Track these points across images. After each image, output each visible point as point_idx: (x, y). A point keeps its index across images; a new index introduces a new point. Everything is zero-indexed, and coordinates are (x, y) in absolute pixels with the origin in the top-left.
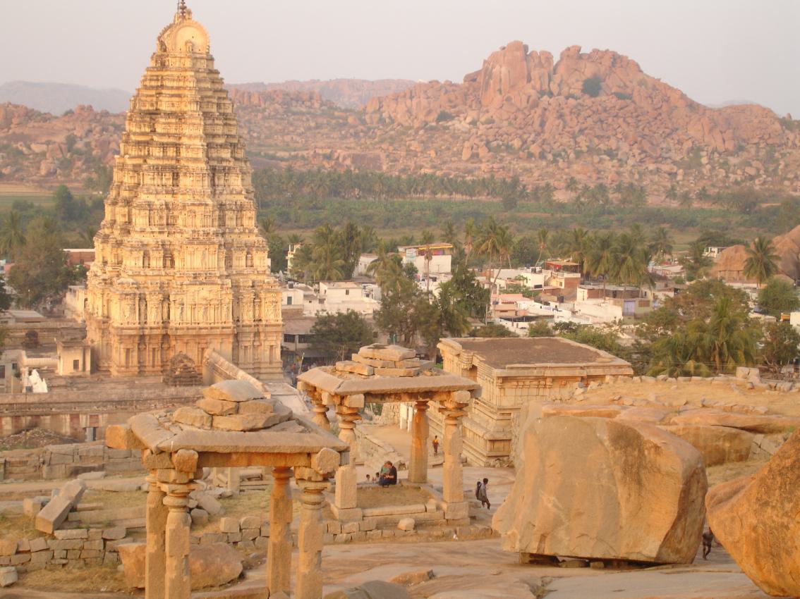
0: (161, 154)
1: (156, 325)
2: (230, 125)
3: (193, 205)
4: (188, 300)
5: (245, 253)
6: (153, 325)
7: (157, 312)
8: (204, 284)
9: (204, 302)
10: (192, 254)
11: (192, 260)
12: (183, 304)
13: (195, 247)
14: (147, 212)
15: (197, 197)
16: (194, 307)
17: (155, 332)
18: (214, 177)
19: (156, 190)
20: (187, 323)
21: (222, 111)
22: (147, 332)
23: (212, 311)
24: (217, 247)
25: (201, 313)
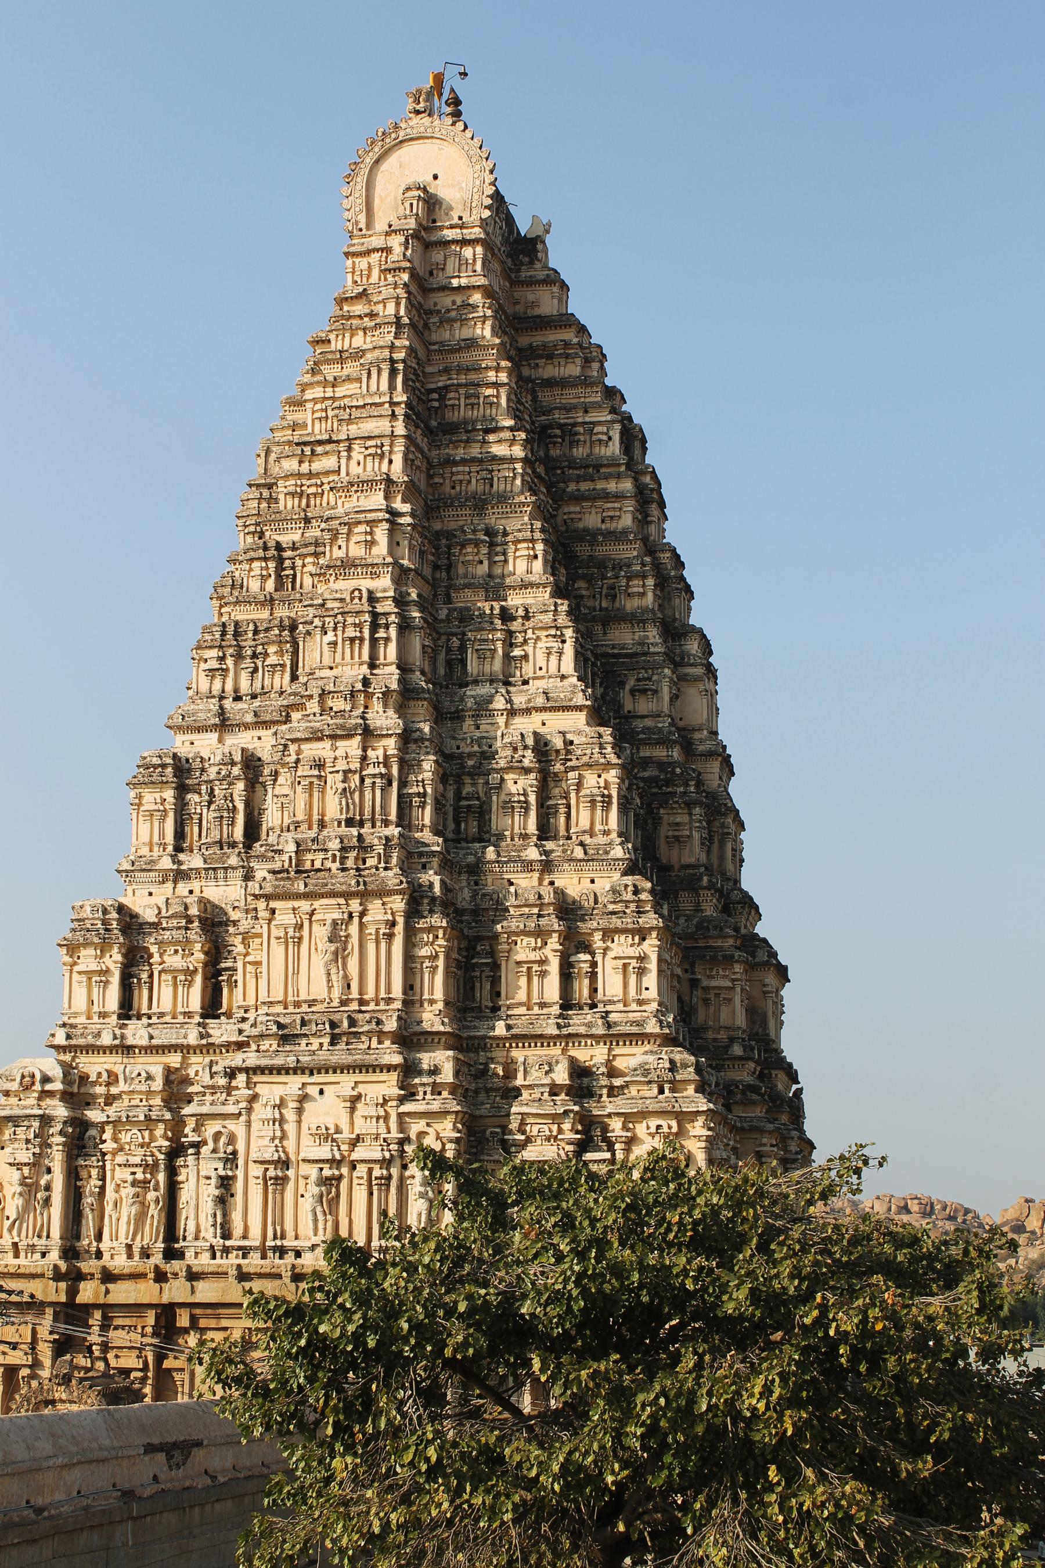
0: (270, 585)
1: (137, 1263)
2: (606, 496)
3: (317, 736)
4: (259, 1144)
5: (554, 942)
6: (120, 1262)
7: (139, 1200)
8: (326, 1069)
9: (325, 1152)
10: (295, 939)
11: (287, 967)
12: (231, 1159)
13: (305, 905)
14: (169, 794)
15: (338, 704)
16: (279, 1171)
17: (122, 1293)
18: (463, 649)
19: (222, 712)
20: (245, 1252)
22: (88, 1292)
23: (360, 1195)
24: (398, 904)
25: (307, 1204)
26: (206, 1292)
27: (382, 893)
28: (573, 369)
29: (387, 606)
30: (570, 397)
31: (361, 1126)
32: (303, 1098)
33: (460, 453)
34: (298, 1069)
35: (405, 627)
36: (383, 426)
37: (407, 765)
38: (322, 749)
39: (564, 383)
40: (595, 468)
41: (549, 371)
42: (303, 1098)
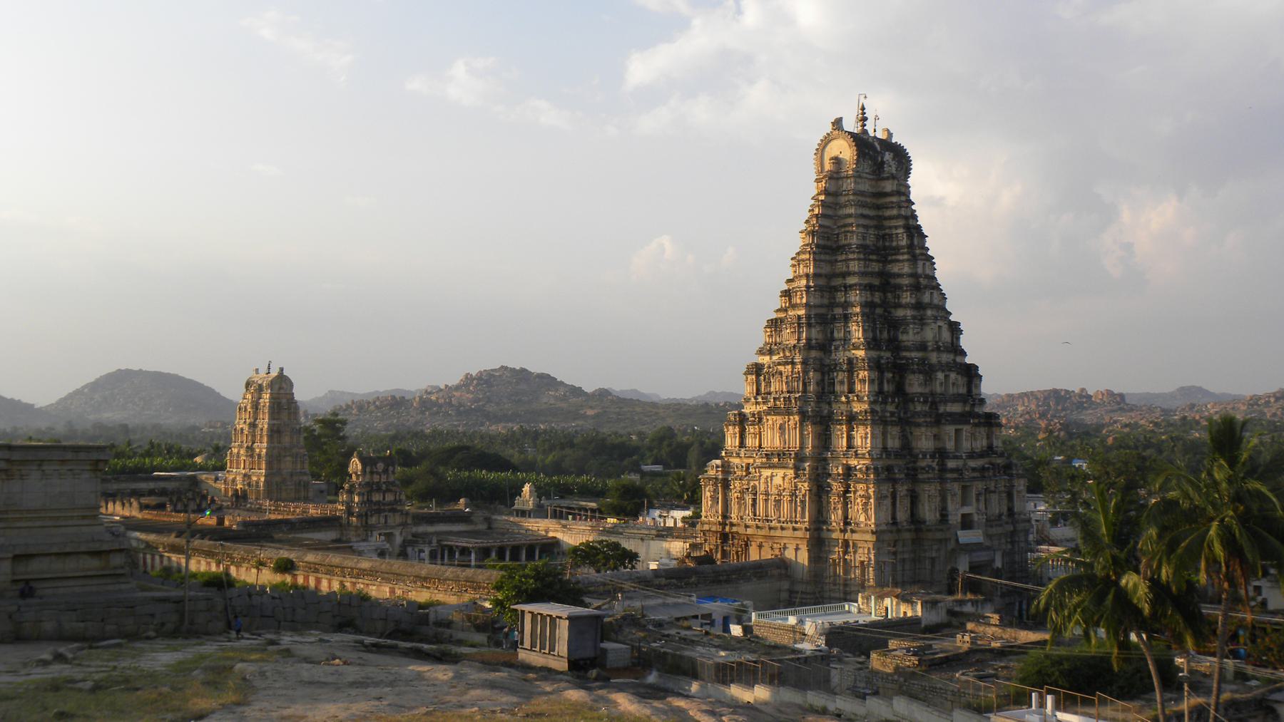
2: (898, 261)
21: (894, 244)
26: (749, 531)
27: (792, 414)
28: (895, 212)
29: (804, 320)
30: (894, 223)
31: (786, 485)
32: (772, 476)
33: (839, 258)
34: (770, 467)
35: (809, 325)
36: (807, 256)
37: (805, 372)
38: (781, 368)
39: (891, 218)
40: (897, 250)
41: (888, 213)
42: (772, 476)
